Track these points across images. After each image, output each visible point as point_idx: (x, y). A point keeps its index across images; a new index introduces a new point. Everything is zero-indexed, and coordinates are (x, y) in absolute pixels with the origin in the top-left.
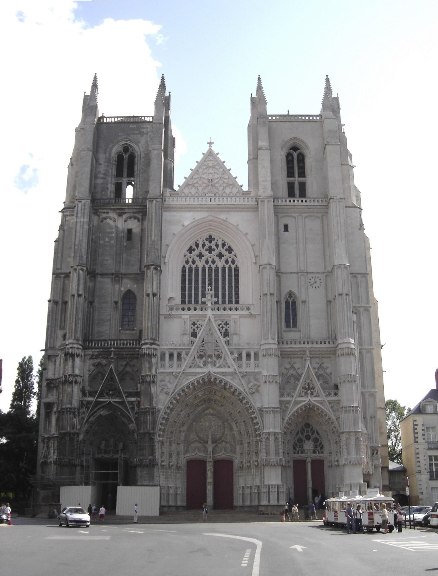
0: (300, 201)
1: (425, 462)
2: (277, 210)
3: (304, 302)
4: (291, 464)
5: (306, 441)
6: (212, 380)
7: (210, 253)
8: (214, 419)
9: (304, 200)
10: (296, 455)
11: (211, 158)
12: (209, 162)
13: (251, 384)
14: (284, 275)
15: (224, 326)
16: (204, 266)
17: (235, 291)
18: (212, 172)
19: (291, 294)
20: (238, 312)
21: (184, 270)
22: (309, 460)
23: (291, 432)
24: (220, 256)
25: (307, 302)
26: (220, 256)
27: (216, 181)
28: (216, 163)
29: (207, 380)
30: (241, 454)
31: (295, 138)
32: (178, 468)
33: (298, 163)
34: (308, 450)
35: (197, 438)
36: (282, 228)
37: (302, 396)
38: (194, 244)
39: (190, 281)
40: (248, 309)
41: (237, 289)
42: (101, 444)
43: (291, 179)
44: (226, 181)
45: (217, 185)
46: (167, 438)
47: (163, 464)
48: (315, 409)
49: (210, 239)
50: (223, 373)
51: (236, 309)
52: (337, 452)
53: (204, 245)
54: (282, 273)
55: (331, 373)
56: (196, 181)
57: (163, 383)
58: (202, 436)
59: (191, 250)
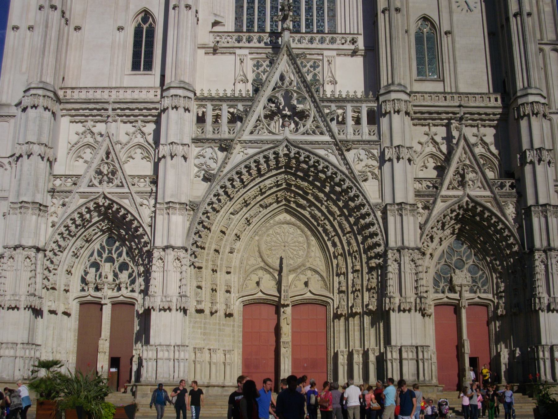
5: (457, 271)
6: (292, 155)
8: (291, 230)
10: (441, 295)
13: (363, 164)
19: (425, 19)
20: (335, 46)
23: (431, 254)
34: (461, 286)
35: (262, 264)
42: (86, 273)
46: (207, 260)
50: (311, 143)
51: (333, 41)
57: (202, 160)
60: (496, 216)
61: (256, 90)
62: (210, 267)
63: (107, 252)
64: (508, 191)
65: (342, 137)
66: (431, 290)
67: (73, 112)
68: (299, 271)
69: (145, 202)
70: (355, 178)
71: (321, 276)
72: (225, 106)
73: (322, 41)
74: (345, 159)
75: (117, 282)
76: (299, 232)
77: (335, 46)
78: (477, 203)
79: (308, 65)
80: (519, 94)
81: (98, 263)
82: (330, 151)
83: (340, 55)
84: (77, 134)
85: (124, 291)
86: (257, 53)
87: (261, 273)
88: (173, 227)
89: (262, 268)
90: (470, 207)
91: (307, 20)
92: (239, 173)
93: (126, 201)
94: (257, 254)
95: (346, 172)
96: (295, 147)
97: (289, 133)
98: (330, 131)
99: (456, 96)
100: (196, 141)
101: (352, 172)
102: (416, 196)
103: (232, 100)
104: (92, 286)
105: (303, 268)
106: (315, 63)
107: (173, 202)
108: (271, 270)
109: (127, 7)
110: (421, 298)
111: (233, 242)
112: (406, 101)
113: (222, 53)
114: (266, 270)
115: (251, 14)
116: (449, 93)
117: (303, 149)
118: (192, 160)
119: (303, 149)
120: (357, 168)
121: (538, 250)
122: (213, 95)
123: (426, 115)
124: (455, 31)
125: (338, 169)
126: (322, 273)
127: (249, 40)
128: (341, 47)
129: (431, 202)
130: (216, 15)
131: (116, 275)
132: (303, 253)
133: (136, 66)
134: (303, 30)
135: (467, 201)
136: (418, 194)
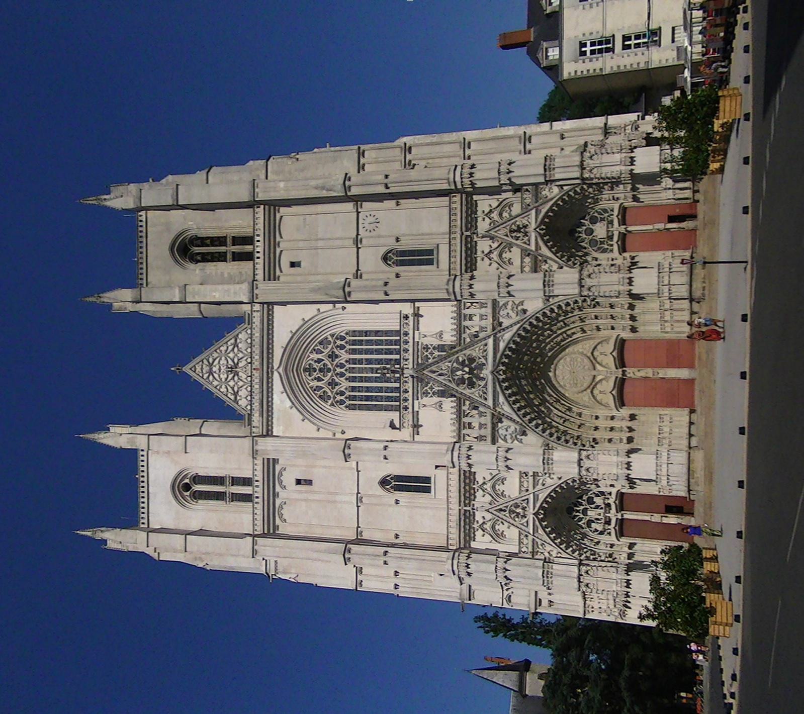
0: (258, 244)
1: (632, 55)
2: (271, 275)
3: (398, 240)
5: (594, 234)
6: (504, 368)
7: (329, 370)
9: (257, 238)
11: (198, 369)
12: (204, 372)
13: (510, 312)
15: (430, 351)
16: (346, 379)
18: (218, 366)
19: (385, 258)
21: (350, 407)
22: (622, 229)
26: (332, 356)
27: (230, 362)
28: (205, 361)
31: (172, 249)
32: (633, 417)
33: (208, 246)
34: (608, 231)
36: (295, 270)
37: (529, 241)
38: (316, 392)
39: (368, 398)
40: (406, 317)
41: (379, 334)
42: (596, 530)
43: (229, 256)
44: (230, 348)
45: (236, 360)
47: (625, 441)
49: (310, 370)
51: (406, 334)
53: (319, 379)
54: (358, 270)
56: (230, 390)
57: (508, 437)
58: (586, 385)
60: (553, 205)
61: (452, 396)
62: (592, 432)
63: (578, 514)
65: (490, 328)
66: (610, 255)
68: (594, 361)
69: (541, 481)
70: (522, 320)
71: (598, 344)
72: (466, 420)
73: (407, 342)
74: (507, 328)
75: (603, 506)
76: (562, 361)
78: (542, 222)
79: (426, 353)
80: (453, 187)
81: (589, 520)
84: (483, 535)
85: (611, 501)
86: (418, 393)
87: (596, 392)
90: (544, 227)
91: (386, 354)
92: (519, 409)
93: (540, 496)
94: (580, 394)
95: (519, 325)
97: (487, 372)
98: (485, 339)
99: (452, 236)
100: (494, 441)
101: (518, 322)
102: (536, 271)
103: (460, 414)
104: (607, 526)
105: (592, 358)
106: (424, 348)
107: (543, 460)
108: (594, 383)
109: (380, 496)
110: (619, 270)
112: (462, 280)
114: (593, 388)
115: (381, 399)
116: (450, 242)
118: (509, 445)
120: (515, 318)
121: (582, 174)
122: (455, 428)
124: (396, 233)
125: (515, 333)
126: (596, 344)
127: (406, 400)
128: (411, 326)
129: (540, 258)
130: (384, 427)
131: (597, 507)
133: (427, 490)
134: (397, 357)
136: (535, 270)
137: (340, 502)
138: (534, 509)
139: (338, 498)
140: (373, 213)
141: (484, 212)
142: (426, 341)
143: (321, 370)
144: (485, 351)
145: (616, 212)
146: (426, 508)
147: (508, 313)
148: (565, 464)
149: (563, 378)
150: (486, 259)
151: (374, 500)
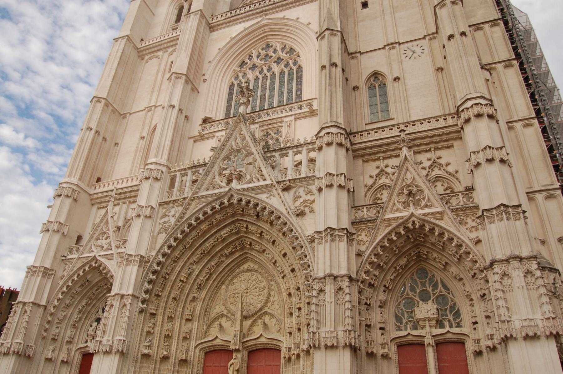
3: (397, 79)
4: (393, 351)
5: (421, 303)
8: (254, 277)
13: (301, 200)
14: (363, 55)
17: (296, 94)
24: (279, 60)
25: (402, 78)
26: (279, 60)
29: (226, 203)
30: (290, 333)
48: (427, 229)
50: (253, 189)
52: (488, 317)
54: (361, 53)
55: (457, 172)
59: (243, 64)
60: (448, 231)
64: (462, 203)
67: (99, 201)
77: (293, 113)
82: (271, 193)
83: (298, 118)
88: (127, 277)
89: (222, 316)
90: (417, 227)
96: (238, 194)
111: (195, 291)
113: (207, 138)
117: (244, 195)
119: (244, 195)
123: (376, 150)
132: (262, 298)
135: (414, 222)
137: (151, 96)
138: (100, 256)
139: (155, 94)
140: (426, 51)
141: (439, 158)
142: (284, 131)
143: (267, 55)
144: (258, 180)
145: (457, 330)
146: (133, 163)
147: (301, 197)
148: (126, 280)
149: (241, 282)
150: (377, 171)
151: (148, 121)
